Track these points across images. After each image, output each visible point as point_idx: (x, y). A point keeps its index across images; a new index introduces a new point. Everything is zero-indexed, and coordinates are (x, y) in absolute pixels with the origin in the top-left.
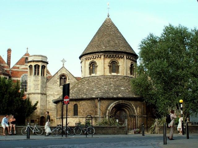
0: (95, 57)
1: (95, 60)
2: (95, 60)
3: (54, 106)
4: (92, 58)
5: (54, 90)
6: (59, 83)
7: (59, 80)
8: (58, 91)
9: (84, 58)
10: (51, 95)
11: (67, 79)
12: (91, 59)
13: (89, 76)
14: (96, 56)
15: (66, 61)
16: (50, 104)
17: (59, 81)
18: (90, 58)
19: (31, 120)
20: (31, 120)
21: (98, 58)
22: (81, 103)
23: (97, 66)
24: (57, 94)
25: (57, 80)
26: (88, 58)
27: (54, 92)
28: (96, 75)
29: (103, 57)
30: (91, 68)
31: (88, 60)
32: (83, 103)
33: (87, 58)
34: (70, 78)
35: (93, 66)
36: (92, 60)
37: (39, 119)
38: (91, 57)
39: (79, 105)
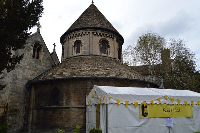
0: (108, 36)
1: (107, 39)
2: (107, 39)
3: (22, 86)
4: (105, 35)
5: (26, 61)
6: (32, 52)
7: (33, 48)
8: (30, 64)
9: (91, 32)
10: (21, 67)
11: (42, 50)
12: (101, 36)
13: (98, 54)
14: (109, 35)
15: (41, 27)
16: (17, 81)
17: (33, 50)
18: (102, 34)
21: (110, 37)
23: (109, 47)
24: (28, 67)
25: (31, 47)
26: (98, 34)
27: (26, 64)
28: (109, 56)
29: (115, 38)
31: (96, 35)
33: (97, 33)
34: (44, 50)
35: (104, 45)
36: (103, 37)
37: (4, 107)
38: (103, 34)
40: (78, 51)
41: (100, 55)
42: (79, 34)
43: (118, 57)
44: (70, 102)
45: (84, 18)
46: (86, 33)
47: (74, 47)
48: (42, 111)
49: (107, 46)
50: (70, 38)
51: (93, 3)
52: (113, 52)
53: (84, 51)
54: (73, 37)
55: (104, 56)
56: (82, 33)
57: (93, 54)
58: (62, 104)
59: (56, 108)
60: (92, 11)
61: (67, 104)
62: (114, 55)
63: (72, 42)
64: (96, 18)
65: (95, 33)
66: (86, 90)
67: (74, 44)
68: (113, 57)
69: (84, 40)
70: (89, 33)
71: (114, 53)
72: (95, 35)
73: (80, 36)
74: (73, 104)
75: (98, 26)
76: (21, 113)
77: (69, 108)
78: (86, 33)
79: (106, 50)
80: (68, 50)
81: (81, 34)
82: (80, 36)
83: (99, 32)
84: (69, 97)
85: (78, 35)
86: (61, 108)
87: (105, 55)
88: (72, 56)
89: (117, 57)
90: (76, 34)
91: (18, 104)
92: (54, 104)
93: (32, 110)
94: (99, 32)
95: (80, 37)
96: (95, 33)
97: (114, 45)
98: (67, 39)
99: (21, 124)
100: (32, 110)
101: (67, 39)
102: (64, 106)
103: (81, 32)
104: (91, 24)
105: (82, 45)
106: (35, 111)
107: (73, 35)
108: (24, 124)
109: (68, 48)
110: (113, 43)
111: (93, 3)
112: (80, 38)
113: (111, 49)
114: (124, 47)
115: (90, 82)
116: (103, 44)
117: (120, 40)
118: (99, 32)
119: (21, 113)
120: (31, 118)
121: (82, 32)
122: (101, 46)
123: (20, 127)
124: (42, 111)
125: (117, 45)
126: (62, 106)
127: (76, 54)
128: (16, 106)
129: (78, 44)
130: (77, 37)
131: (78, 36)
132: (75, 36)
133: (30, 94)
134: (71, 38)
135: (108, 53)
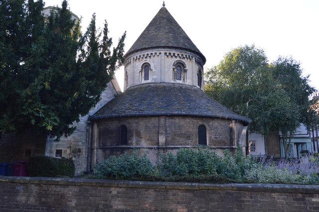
0: (184, 56)
1: (183, 60)
2: (183, 60)
4: (180, 56)
9: (163, 51)
12: (176, 57)
13: (172, 81)
18: (176, 55)
19: (56, 150)
20: (56, 150)
22: (211, 123)
23: (185, 71)
26: (172, 55)
29: (194, 59)
30: (176, 70)
32: (216, 123)
33: (170, 54)
35: (180, 67)
36: (178, 59)
39: (207, 128)
40: (146, 77)
41: (174, 82)
42: (148, 54)
43: (197, 84)
44: (140, 141)
45: (153, 32)
46: (156, 53)
47: (141, 71)
48: (108, 151)
49: (183, 71)
50: (136, 60)
51: (164, 5)
52: (191, 77)
53: (154, 77)
54: (139, 59)
55: (179, 84)
56: (152, 54)
57: (166, 82)
58: (131, 144)
59: (123, 148)
60: (164, 20)
61: (137, 144)
62: (193, 81)
63: (139, 65)
64: (170, 32)
65: (168, 54)
66: (159, 128)
67: (140, 68)
68: (191, 85)
69: (153, 62)
70: (160, 53)
71: (192, 79)
72: (168, 56)
73: (148, 58)
74: (144, 144)
75: (171, 45)
76: (84, 153)
77: (139, 148)
78: (156, 53)
79: (182, 76)
80: (133, 75)
81: (150, 55)
82: (148, 58)
83: (173, 52)
84: (138, 135)
85: (145, 56)
86: (130, 148)
87: (181, 82)
88: (139, 83)
89: (196, 84)
90: (144, 55)
91: (80, 143)
92: (122, 144)
93: (96, 150)
94: (173, 52)
95: (148, 58)
96: (168, 54)
97: (192, 68)
98: (132, 60)
99: (85, 166)
100: (96, 150)
101: (132, 60)
102: (134, 146)
103: (149, 52)
104: (164, 42)
105: (151, 70)
106: (100, 152)
107: (140, 56)
108: (87, 164)
109: (134, 72)
110: (191, 66)
111: (164, 5)
112: (148, 60)
113: (189, 74)
114: (207, 67)
115: (163, 120)
116: (178, 67)
117: (201, 60)
118: (173, 52)
119: (84, 153)
120: (95, 160)
121: (151, 52)
122: (176, 70)
123: (83, 169)
124: (108, 152)
125: (196, 68)
126: (131, 146)
127: (144, 82)
128: (79, 145)
129: (146, 67)
130: (144, 59)
131: (146, 57)
132: (143, 58)
133: (92, 131)
134: (137, 60)
135: (184, 80)
